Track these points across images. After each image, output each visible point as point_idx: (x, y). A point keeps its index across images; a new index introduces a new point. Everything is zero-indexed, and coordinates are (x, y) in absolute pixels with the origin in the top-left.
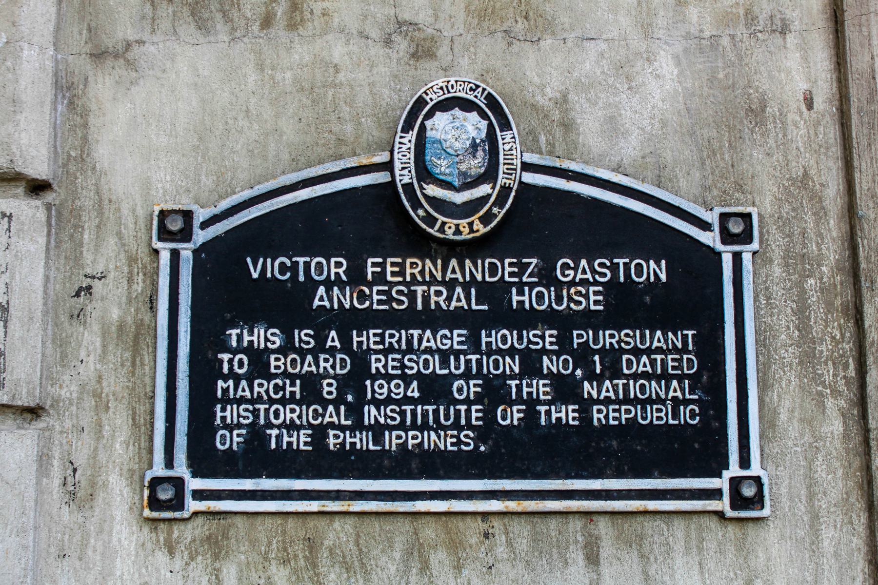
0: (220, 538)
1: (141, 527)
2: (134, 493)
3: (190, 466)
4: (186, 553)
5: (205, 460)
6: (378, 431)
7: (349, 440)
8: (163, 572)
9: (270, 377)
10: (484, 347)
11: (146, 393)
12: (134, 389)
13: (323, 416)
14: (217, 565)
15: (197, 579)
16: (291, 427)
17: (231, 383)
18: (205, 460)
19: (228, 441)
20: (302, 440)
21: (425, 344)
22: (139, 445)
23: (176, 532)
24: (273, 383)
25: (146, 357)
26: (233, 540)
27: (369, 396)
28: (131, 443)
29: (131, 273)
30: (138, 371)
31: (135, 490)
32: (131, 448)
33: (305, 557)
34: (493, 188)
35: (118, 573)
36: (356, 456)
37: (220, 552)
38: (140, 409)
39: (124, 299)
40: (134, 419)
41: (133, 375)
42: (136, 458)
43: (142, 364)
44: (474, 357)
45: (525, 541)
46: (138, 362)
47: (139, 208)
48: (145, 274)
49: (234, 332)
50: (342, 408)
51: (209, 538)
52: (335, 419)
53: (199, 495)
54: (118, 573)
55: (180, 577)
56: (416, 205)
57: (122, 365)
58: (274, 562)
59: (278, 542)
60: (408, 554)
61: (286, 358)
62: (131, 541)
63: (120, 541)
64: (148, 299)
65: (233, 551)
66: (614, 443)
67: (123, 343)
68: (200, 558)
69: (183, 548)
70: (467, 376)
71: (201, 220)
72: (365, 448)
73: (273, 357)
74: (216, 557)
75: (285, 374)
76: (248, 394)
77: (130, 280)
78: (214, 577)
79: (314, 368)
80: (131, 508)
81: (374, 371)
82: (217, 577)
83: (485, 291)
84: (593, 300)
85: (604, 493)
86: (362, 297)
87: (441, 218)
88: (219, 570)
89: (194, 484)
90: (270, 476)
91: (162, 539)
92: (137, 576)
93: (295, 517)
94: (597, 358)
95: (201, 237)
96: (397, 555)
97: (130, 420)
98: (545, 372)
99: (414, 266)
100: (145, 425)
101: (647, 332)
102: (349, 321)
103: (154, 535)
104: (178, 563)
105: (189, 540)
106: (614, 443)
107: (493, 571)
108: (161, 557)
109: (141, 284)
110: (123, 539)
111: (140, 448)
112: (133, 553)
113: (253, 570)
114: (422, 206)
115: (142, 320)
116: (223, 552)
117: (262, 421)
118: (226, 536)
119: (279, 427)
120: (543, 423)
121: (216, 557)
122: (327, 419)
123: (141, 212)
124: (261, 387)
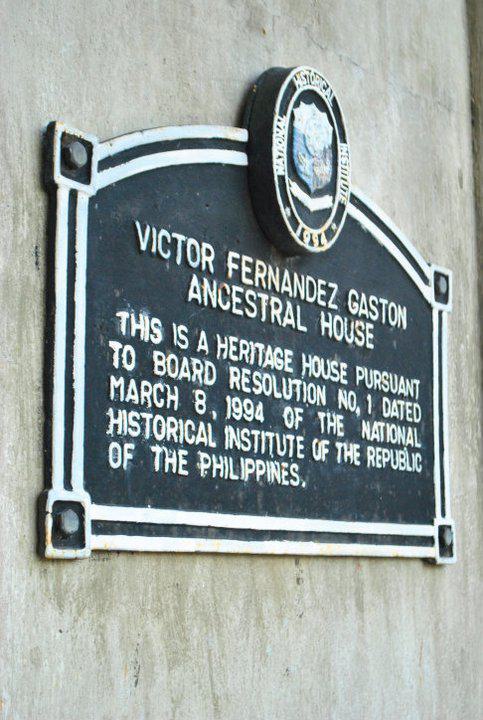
0: (104, 584)
1: (31, 570)
2: (24, 522)
3: (87, 488)
4: (74, 605)
5: (104, 484)
6: (236, 454)
7: (216, 466)
8: (52, 632)
9: (154, 379)
10: (304, 373)
11: (33, 383)
12: (20, 374)
13: (196, 434)
14: (102, 620)
15: (84, 640)
16: (171, 444)
17: (122, 380)
18: (104, 484)
19: (120, 457)
20: (176, 462)
21: (267, 362)
22: (28, 455)
23: (65, 577)
24: (156, 386)
25: (32, 330)
26: (116, 586)
27: (229, 416)
28: (20, 450)
29: (16, 208)
30: (25, 352)
31: (24, 517)
32: (19, 457)
33: (175, 608)
34: (334, 201)
35: (9, 636)
36: (220, 485)
37: (105, 603)
38: (27, 404)
39: (9, 243)
40: (21, 416)
41: (20, 355)
42: (25, 472)
43: (29, 341)
44: (298, 382)
45: (322, 587)
46: (24, 338)
47: (23, 120)
48: (30, 215)
49: (123, 315)
50: (209, 425)
51: (94, 584)
52: (204, 440)
53: (102, 528)
54: (9, 636)
55: (69, 639)
56: (287, 203)
57: (9, 338)
58: (150, 615)
59: (153, 589)
60: (248, 602)
61: (166, 357)
62: (21, 591)
63: (9, 590)
64: (33, 250)
65: (116, 602)
66: (378, 487)
67: (9, 306)
68: (87, 611)
69: (71, 599)
70: (293, 403)
71: (99, 159)
72: (226, 477)
73: (156, 354)
74: (101, 610)
75: (167, 379)
76: (135, 398)
77: (16, 220)
78: (99, 637)
79: (188, 375)
80: (20, 543)
81: (232, 387)
82: (102, 637)
83: (311, 312)
84: (366, 340)
85: (379, 538)
86: (226, 296)
87: (302, 225)
88: (102, 627)
89: (95, 512)
90: (156, 506)
91: (51, 587)
92: (27, 639)
93: (156, 556)
94: (369, 397)
95: (102, 179)
96: (241, 603)
97: (18, 418)
98: (340, 407)
99: (266, 272)
100: (33, 426)
101: (396, 377)
102: (217, 322)
103: (43, 581)
104: (67, 619)
105: (76, 588)
106: (378, 487)
107: (303, 619)
108: (51, 612)
109: (26, 227)
110: (13, 587)
111: (28, 459)
112: (24, 607)
113: (133, 625)
114: (289, 206)
115: (28, 278)
116: (108, 602)
117: (147, 436)
118: (108, 580)
119: (160, 443)
120: (339, 462)
121: (101, 610)
122: (199, 440)
123: (27, 126)
124: (149, 391)
